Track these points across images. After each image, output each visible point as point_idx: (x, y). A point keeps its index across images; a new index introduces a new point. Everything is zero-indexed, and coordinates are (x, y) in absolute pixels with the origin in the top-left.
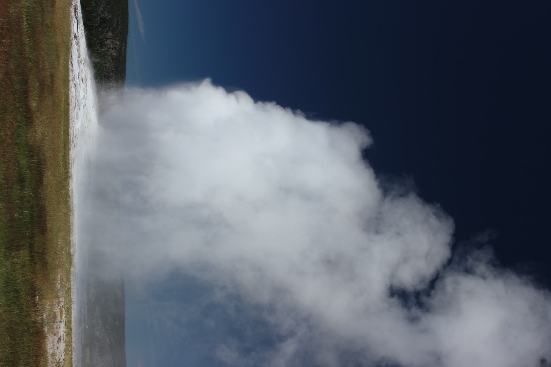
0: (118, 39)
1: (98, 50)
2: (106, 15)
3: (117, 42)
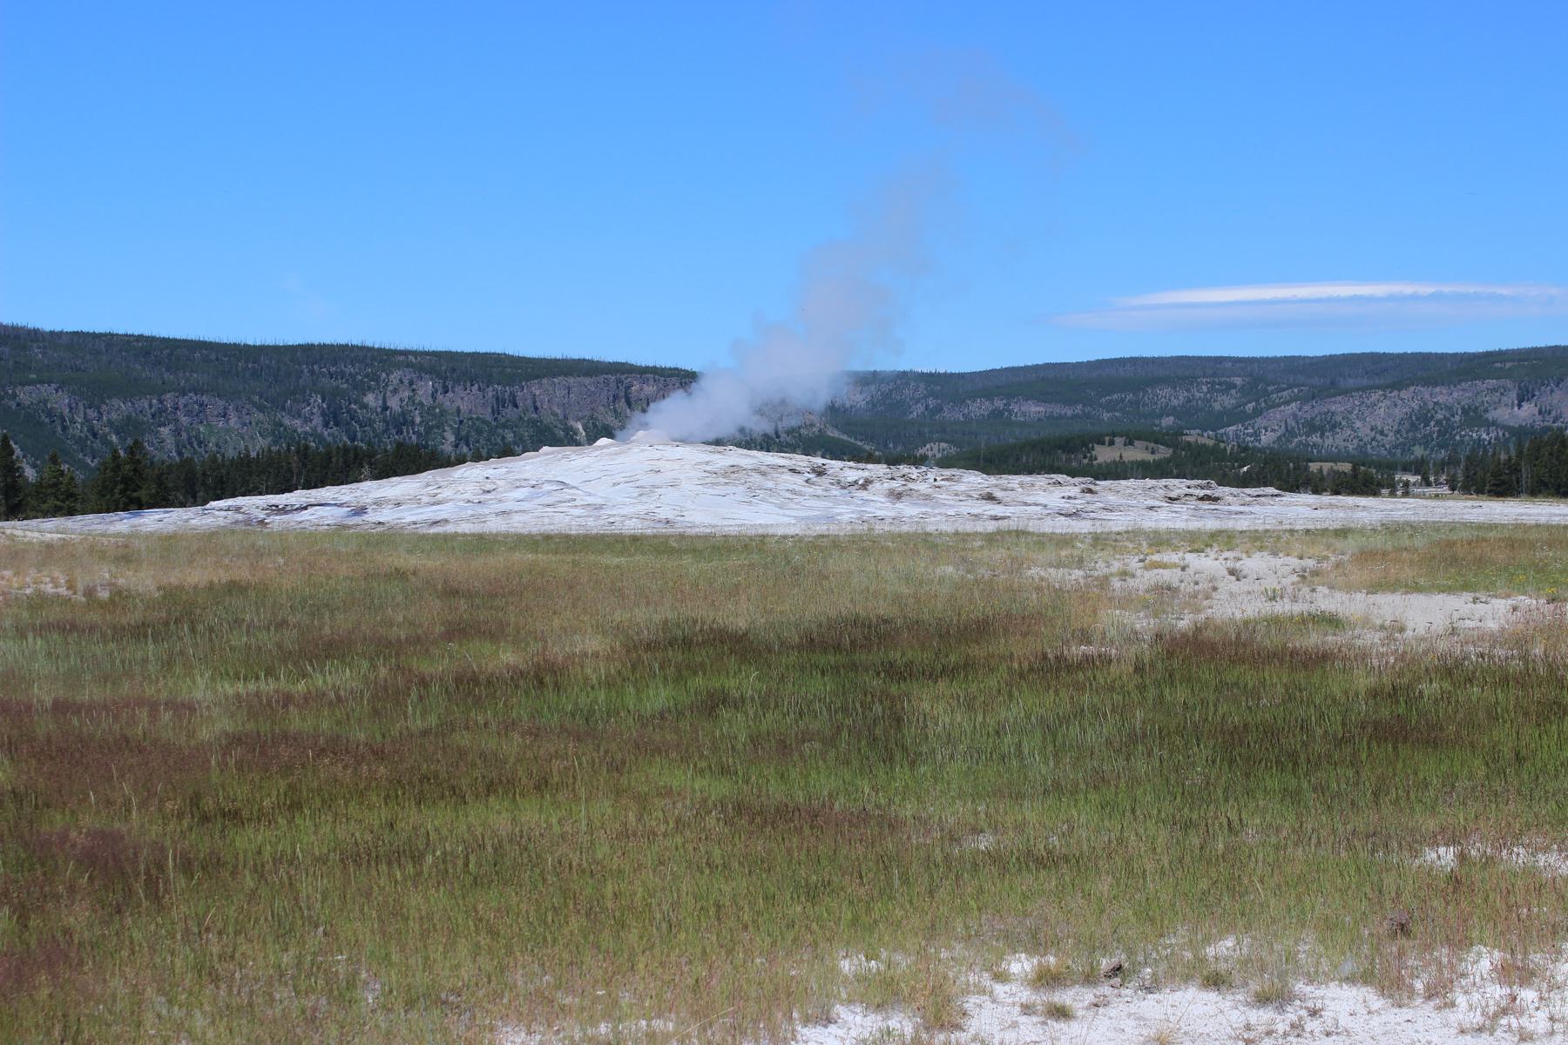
0: (384, 375)
1: (419, 434)
2: (315, 410)
3: (395, 377)
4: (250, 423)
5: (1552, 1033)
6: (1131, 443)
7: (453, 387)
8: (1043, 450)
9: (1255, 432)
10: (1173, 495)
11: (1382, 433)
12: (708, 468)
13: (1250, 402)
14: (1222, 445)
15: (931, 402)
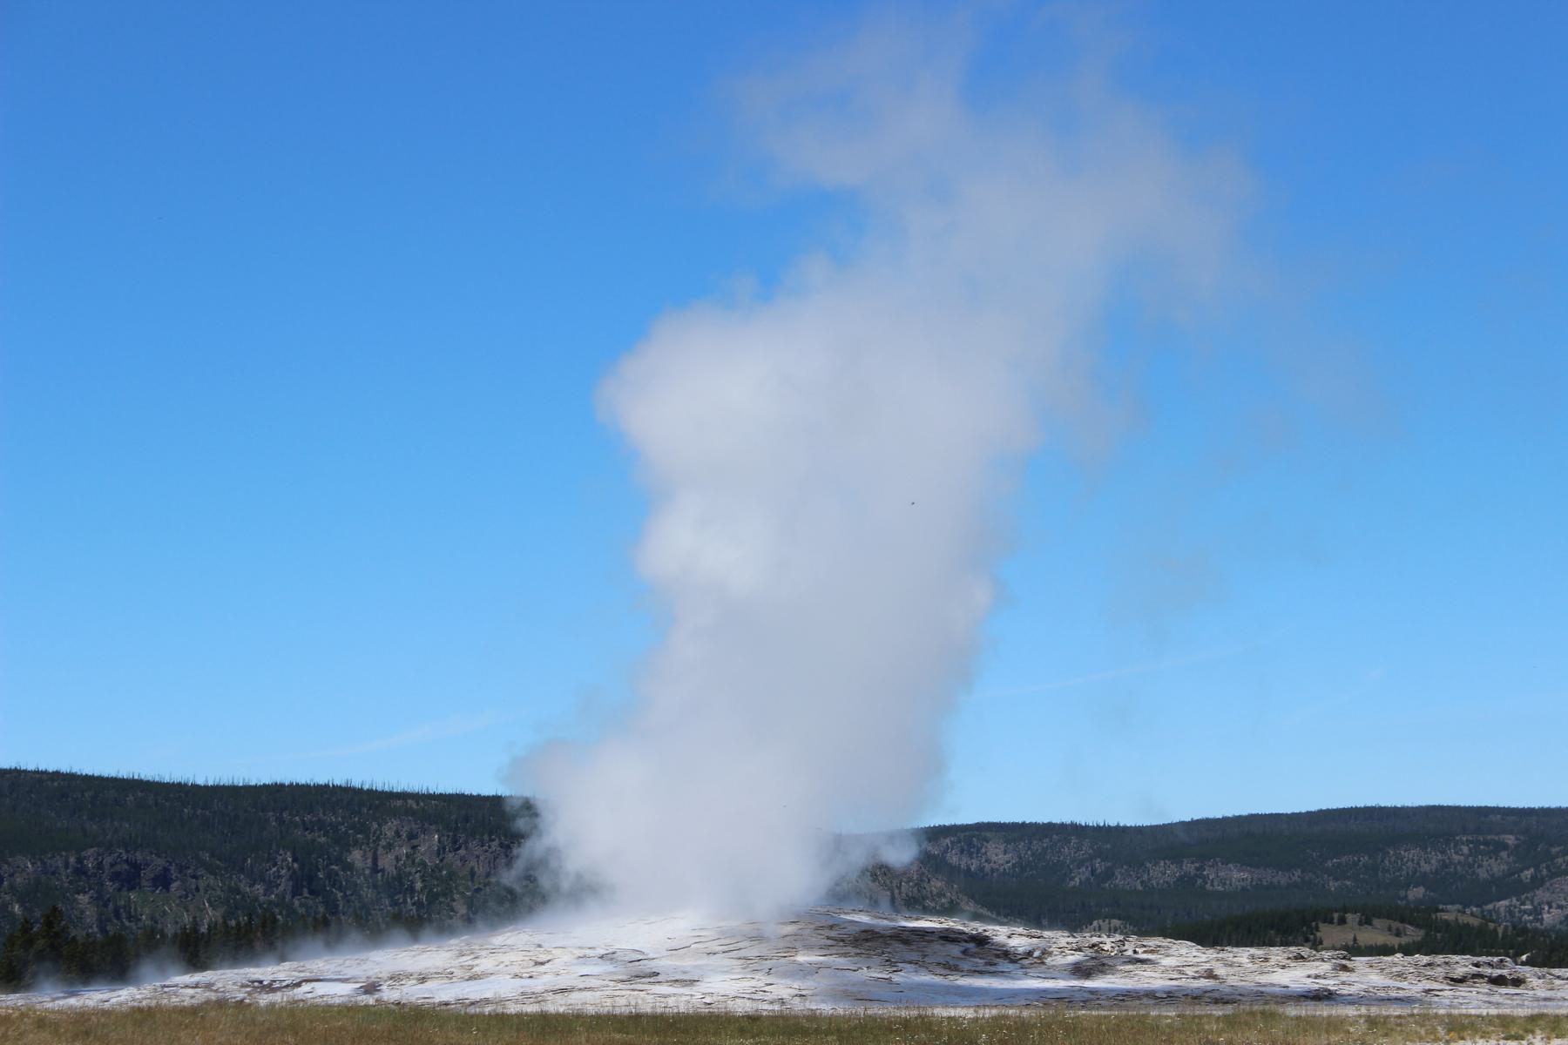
0: (375, 826)
1: (419, 904)
2: (283, 872)
3: (389, 829)
4: (197, 889)
6: (1369, 922)
7: (466, 842)
8: (1249, 931)
9: (1535, 908)
10: (1460, 971)
12: (833, 934)
13: (1528, 869)
14: (1491, 925)
15: (1099, 865)
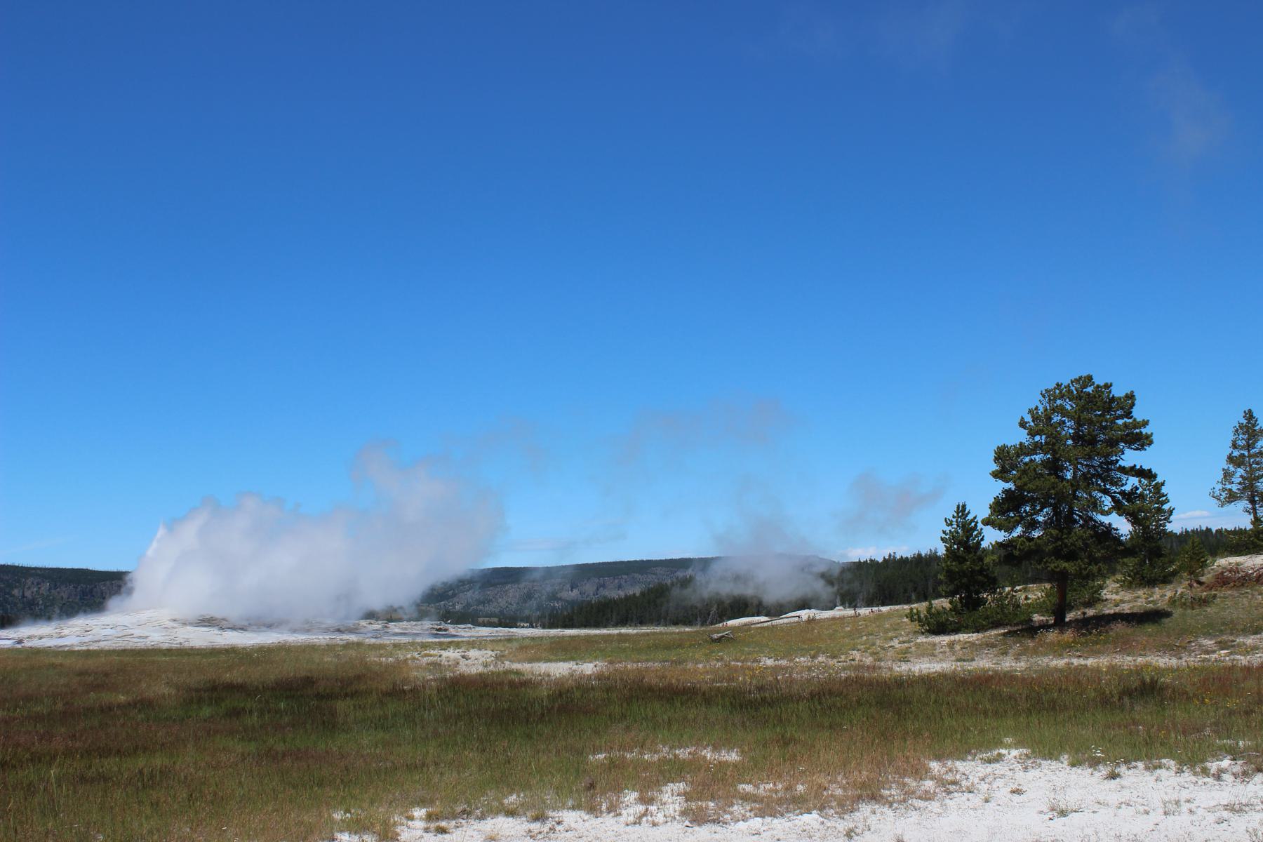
0: (24, 580)
3: (29, 581)
5: (666, 822)
11: (511, 604)
